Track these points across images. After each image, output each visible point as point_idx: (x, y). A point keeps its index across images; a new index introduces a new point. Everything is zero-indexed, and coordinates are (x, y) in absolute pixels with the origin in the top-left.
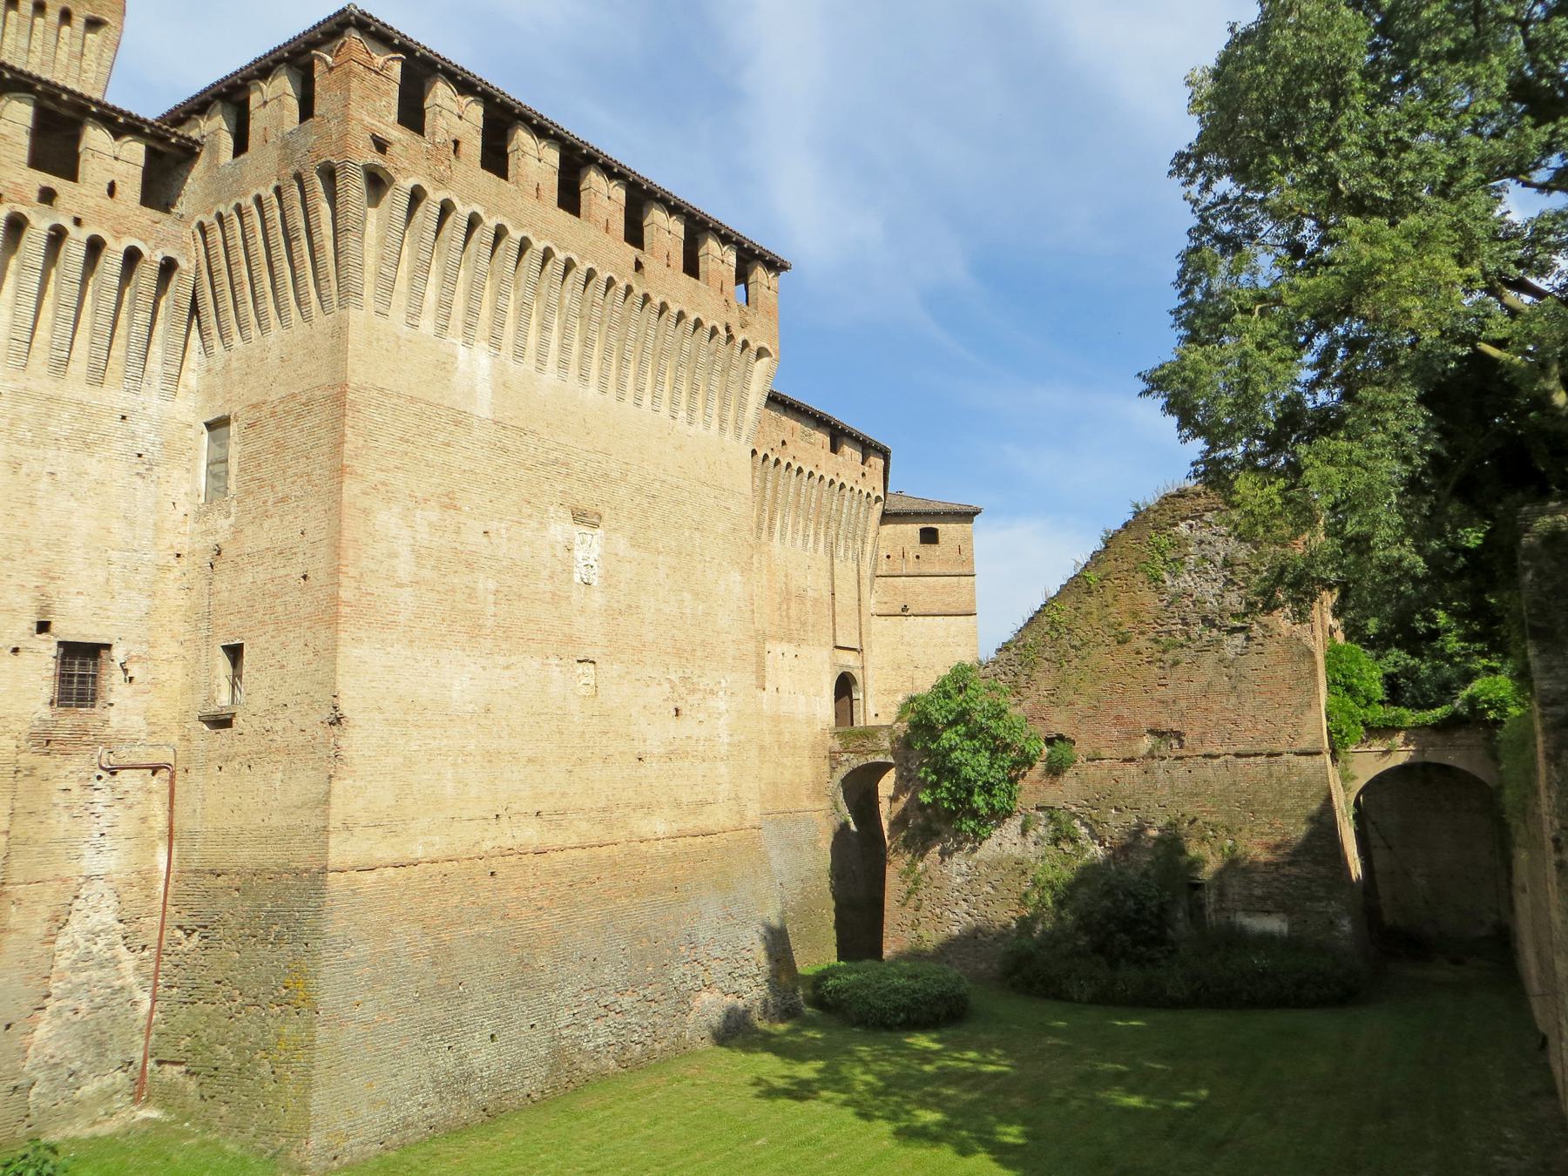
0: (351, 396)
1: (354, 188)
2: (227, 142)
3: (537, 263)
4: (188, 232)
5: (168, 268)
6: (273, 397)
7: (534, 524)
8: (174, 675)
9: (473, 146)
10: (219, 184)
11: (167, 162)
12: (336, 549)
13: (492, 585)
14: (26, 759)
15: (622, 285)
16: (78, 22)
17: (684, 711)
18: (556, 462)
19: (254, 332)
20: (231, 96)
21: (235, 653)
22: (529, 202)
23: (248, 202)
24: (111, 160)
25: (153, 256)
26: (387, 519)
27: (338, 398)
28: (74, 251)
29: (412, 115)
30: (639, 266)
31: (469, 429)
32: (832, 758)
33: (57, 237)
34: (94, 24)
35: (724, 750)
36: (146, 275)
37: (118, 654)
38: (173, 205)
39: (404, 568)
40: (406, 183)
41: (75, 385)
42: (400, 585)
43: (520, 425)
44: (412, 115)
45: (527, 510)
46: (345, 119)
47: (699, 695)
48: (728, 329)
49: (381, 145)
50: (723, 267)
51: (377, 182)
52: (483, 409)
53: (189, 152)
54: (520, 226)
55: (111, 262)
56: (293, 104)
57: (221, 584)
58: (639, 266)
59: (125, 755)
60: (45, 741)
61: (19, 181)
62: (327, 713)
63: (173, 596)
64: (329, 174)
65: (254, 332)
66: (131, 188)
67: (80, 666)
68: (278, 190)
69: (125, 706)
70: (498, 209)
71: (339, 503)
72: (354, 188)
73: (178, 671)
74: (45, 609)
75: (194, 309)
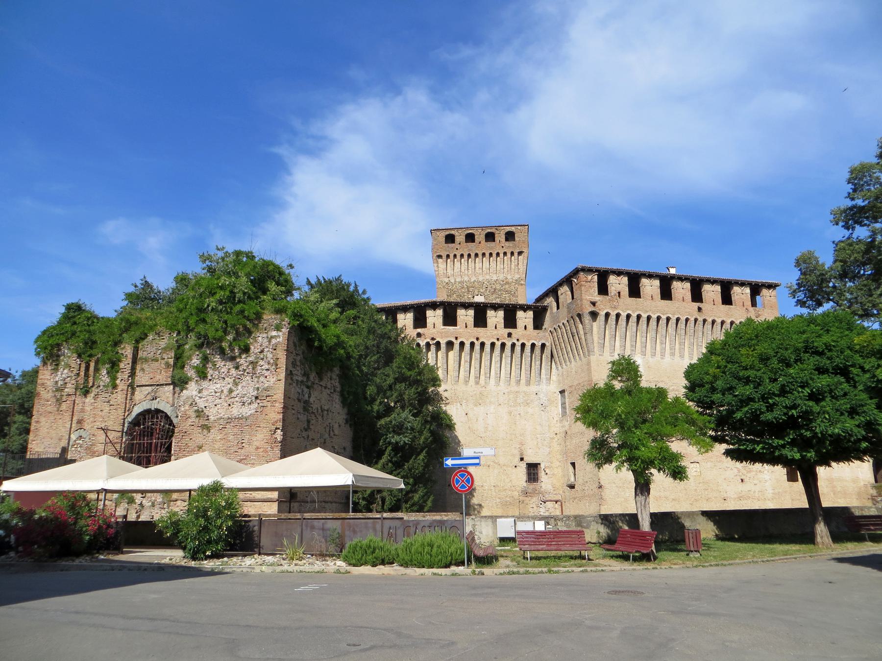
1: (587, 319)
2: (555, 304)
3: (655, 323)
4: (547, 334)
5: (543, 346)
8: (559, 472)
9: (625, 291)
10: (555, 319)
11: (539, 314)
14: (521, 498)
15: (692, 319)
16: (516, 254)
17: (746, 480)
19: (568, 363)
20: (553, 292)
21: (573, 464)
22: (649, 302)
23: (561, 325)
24: (525, 318)
25: (538, 344)
28: (518, 348)
29: (603, 289)
30: (700, 309)
32: (873, 499)
33: (513, 345)
34: (520, 253)
35: (770, 496)
36: (538, 350)
37: (542, 466)
38: (543, 325)
40: (603, 313)
41: (523, 387)
44: (603, 289)
46: (581, 300)
47: (754, 473)
49: (594, 304)
50: (743, 296)
51: (594, 315)
53: (545, 309)
55: (528, 349)
56: (569, 293)
57: (568, 444)
59: (548, 497)
60: (526, 493)
63: (556, 447)
64: (579, 316)
65: (568, 363)
66: (530, 326)
67: (533, 470)
69: (546, 482)
70: (637, 309)
72: (587, 319)
73: (560, 470)
74: (521, 454)
75: (552, 356)
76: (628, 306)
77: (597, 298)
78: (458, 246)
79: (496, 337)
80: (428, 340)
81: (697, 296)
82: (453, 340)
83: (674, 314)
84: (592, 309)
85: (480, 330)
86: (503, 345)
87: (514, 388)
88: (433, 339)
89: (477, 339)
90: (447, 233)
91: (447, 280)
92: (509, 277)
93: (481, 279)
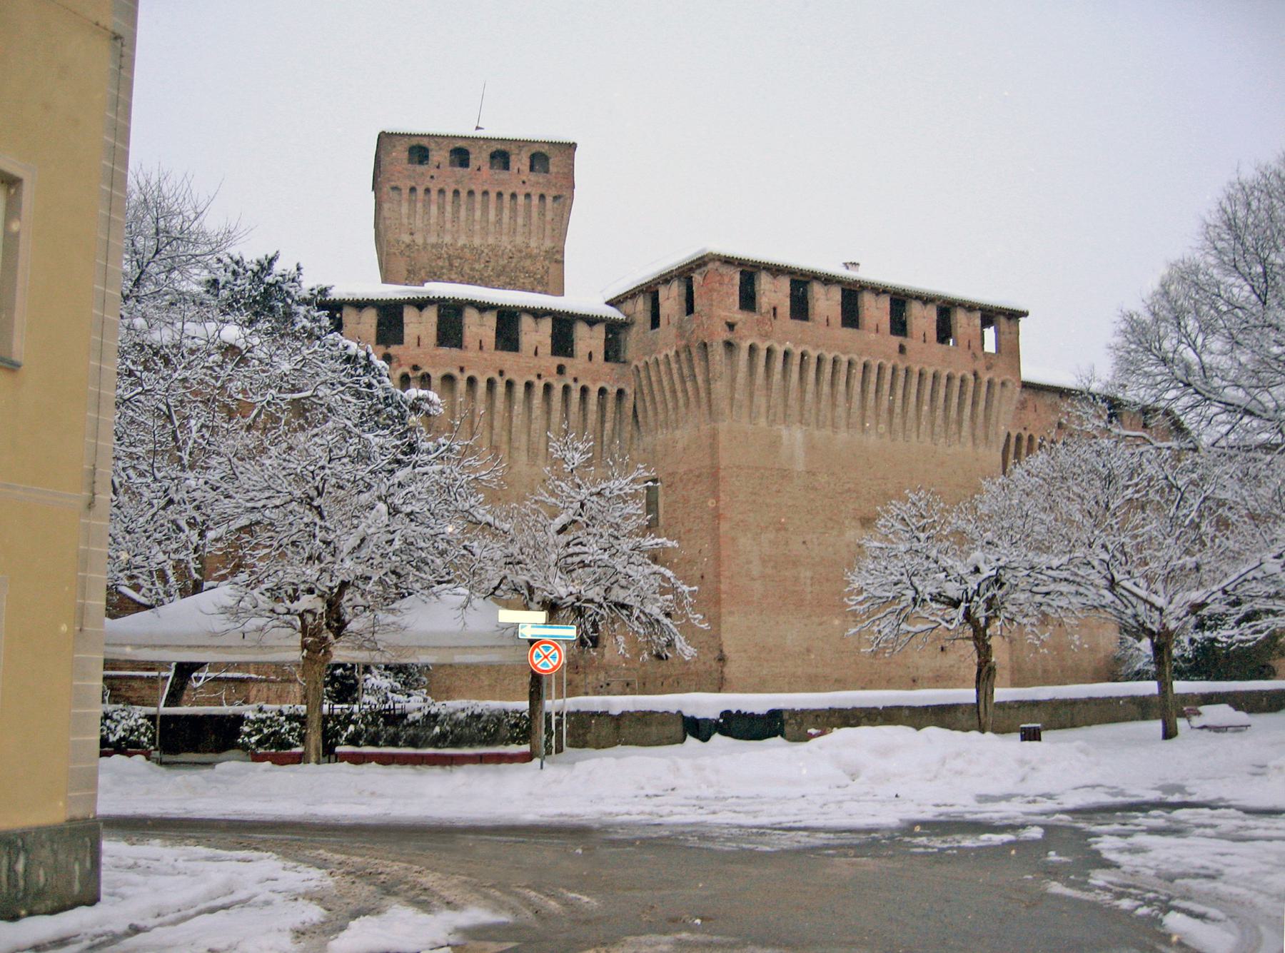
0: (722, 474)
1: (718, 352)
5: (620, 393)
6: (681, 471)
7: (835, 533)
12: (717, 559)
13: (809, 574)
18: (849, 490)
25: (612, 390)
26: (745, 541)
27: (715, 474)
28: (575, 395)
29: (748, 300)
30: (902, 349)
39: (756, 570)
40: (745, 345)
42: (753, 579)
44: (748, 300)
45: (830, 524)
46: (710, 317)
48: (975, 374)
49: (731, 326)
52: (800, 466)
54: (817, 347)
58: (902, 349)
62: (717, 654)
68: (677, 353)
70: (802, 341)
71: (718, 536)
72: (718, 352)
76: (788, 336)
77: (738, 316)
78: (434, 172)
79: (535, 372)
80: (407, 369)
81: (899, 326)
82: (456, 372)
83: (860, 355)
84: (726, 335)
85: (507, 358)
86: (548, 388)
88: (415, 368)
89: (501, 373)
90: (414, 142)
91: (406, 238)
92: (533, 244)
93: (477, 241)
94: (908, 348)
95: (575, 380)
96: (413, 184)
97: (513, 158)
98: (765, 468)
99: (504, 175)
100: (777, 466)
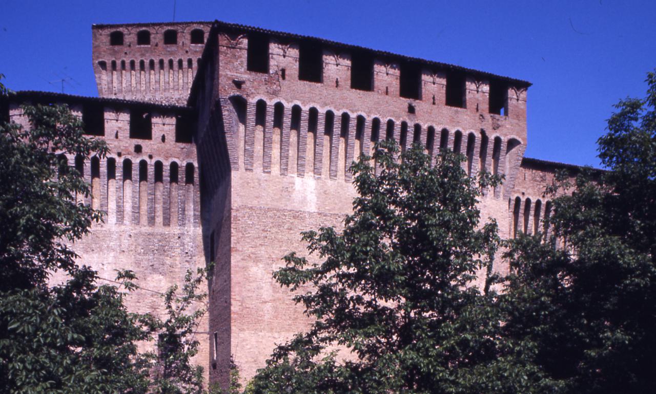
30: (411, 110)
31: (303, 219)
43: (336, 212)
50: (479, 96)
52: (313, 208)
58: (411, 110)
61: (127, 145)
83: (369, 114)
87: (146, 229)
94: (417, 109)
95: (151, 157)
96: (114, 59)
97: (179, 35)
98: (278, 211)
99: (173, 48)
100: (289, 208)
